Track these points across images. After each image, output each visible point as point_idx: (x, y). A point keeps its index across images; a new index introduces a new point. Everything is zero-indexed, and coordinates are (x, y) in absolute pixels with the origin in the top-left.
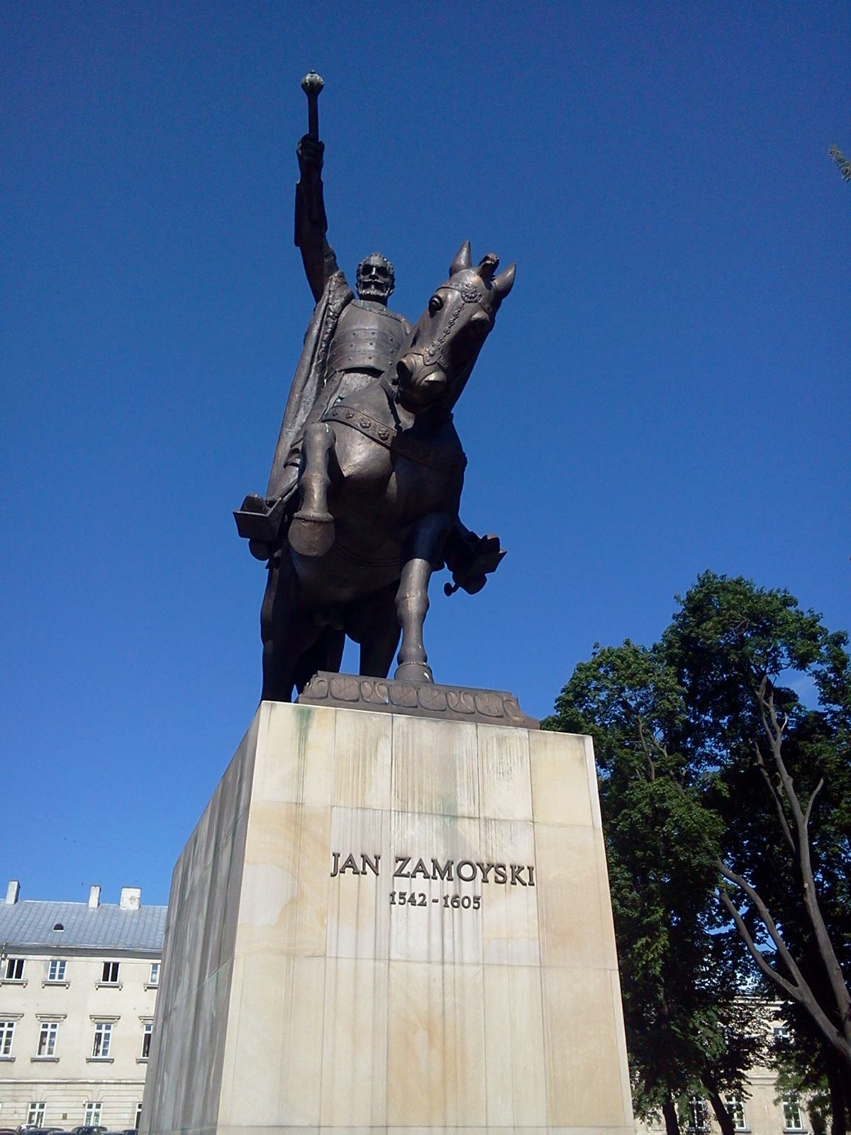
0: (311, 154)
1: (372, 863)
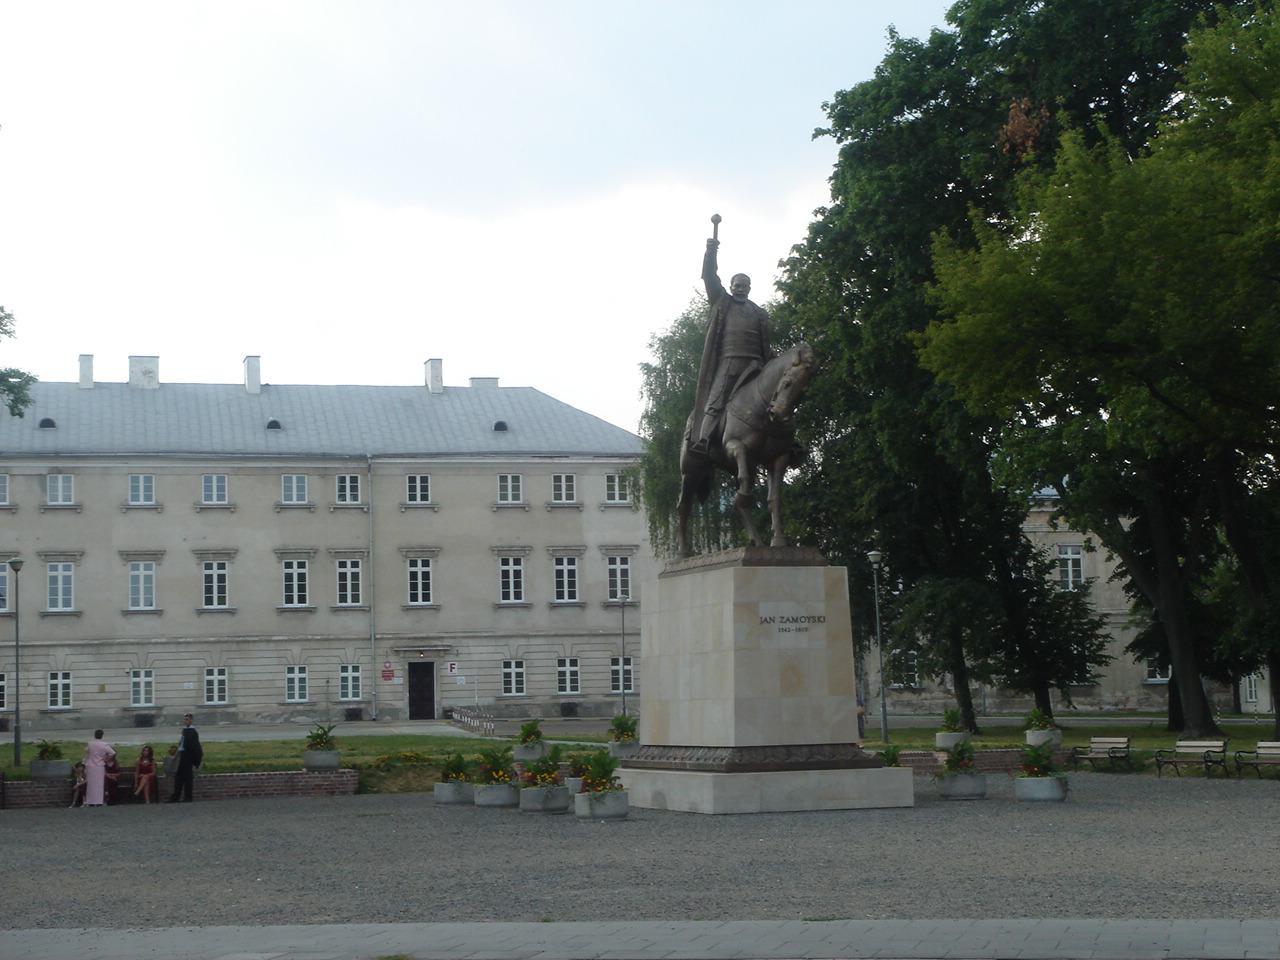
1: (772, 620)
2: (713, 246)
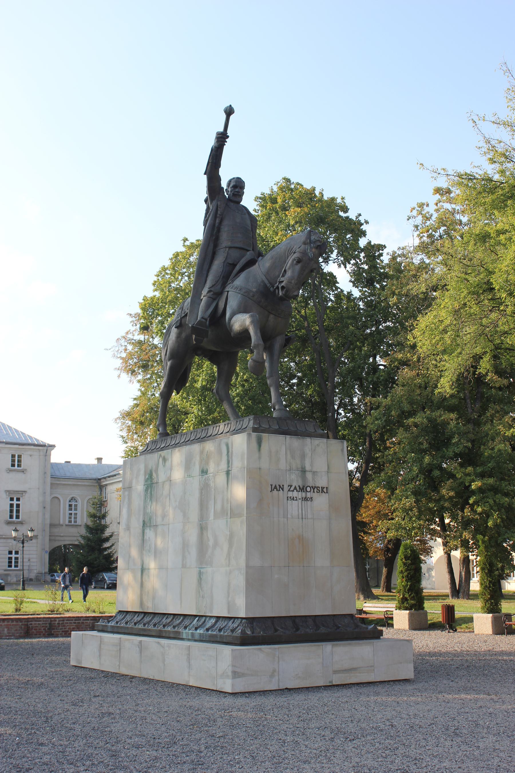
2: (222, 138)
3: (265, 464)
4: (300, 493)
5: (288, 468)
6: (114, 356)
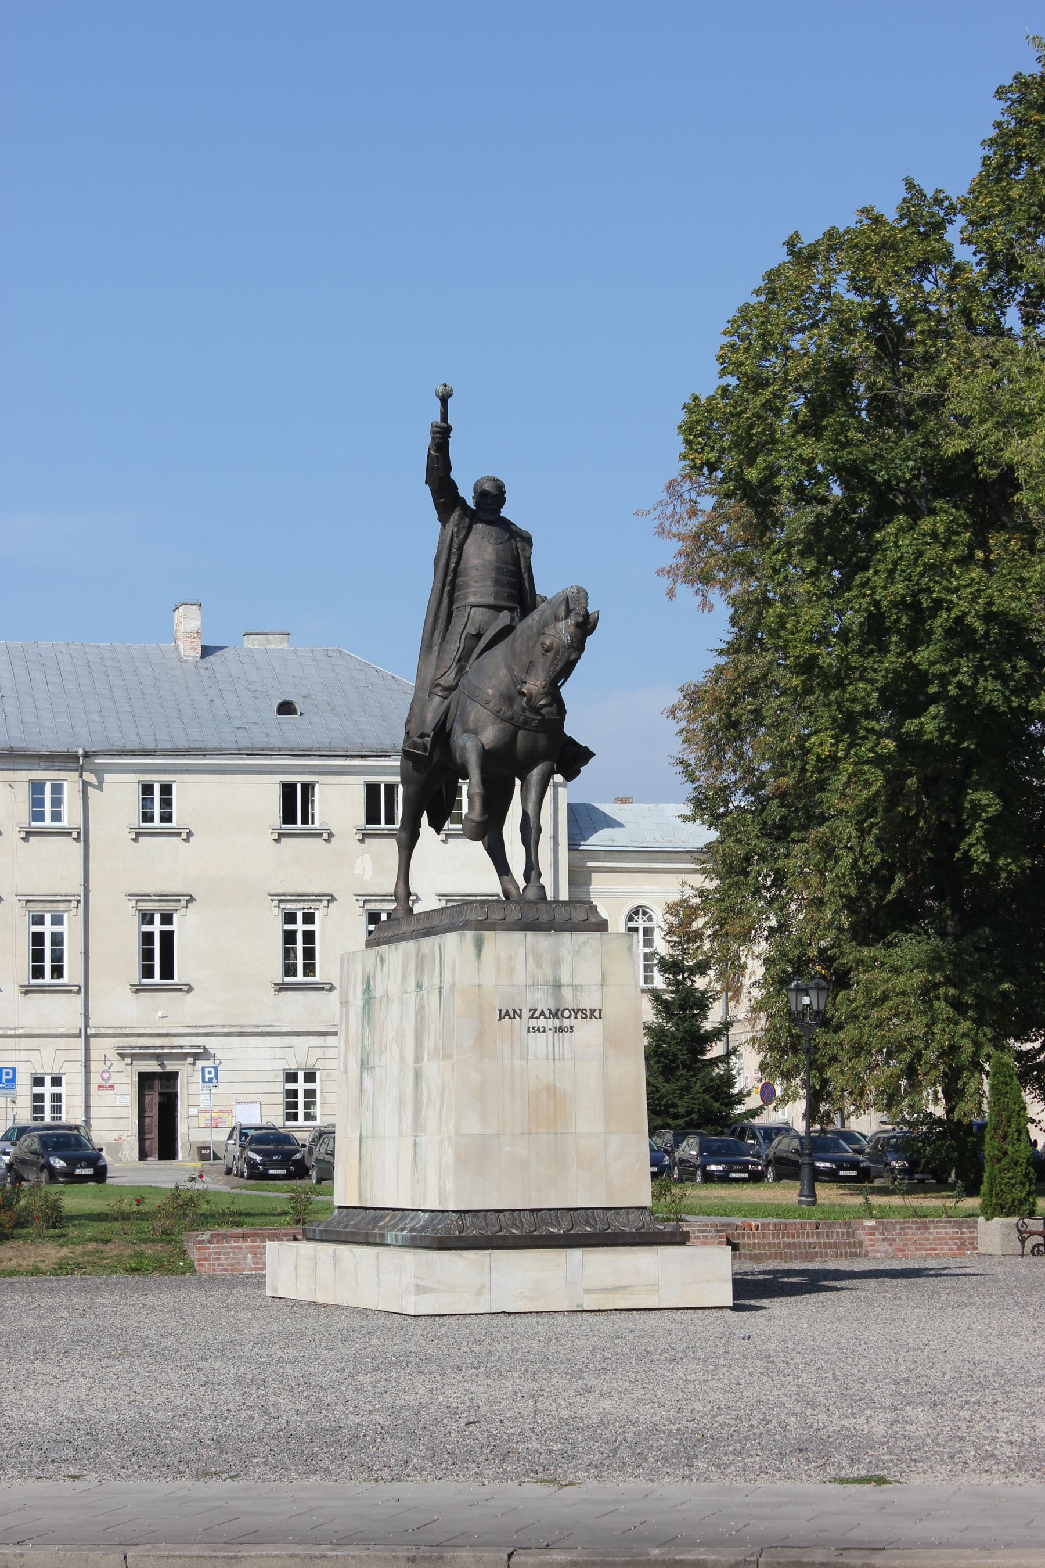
0: (442, 436)
3: (488, 978)
4: (550, 1021)
5: (530, 982)
6: (661, 530)
